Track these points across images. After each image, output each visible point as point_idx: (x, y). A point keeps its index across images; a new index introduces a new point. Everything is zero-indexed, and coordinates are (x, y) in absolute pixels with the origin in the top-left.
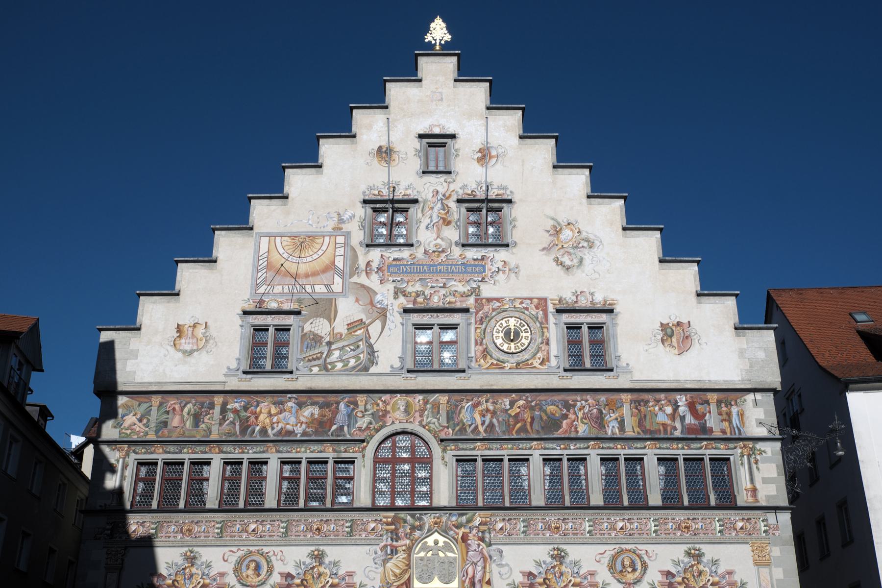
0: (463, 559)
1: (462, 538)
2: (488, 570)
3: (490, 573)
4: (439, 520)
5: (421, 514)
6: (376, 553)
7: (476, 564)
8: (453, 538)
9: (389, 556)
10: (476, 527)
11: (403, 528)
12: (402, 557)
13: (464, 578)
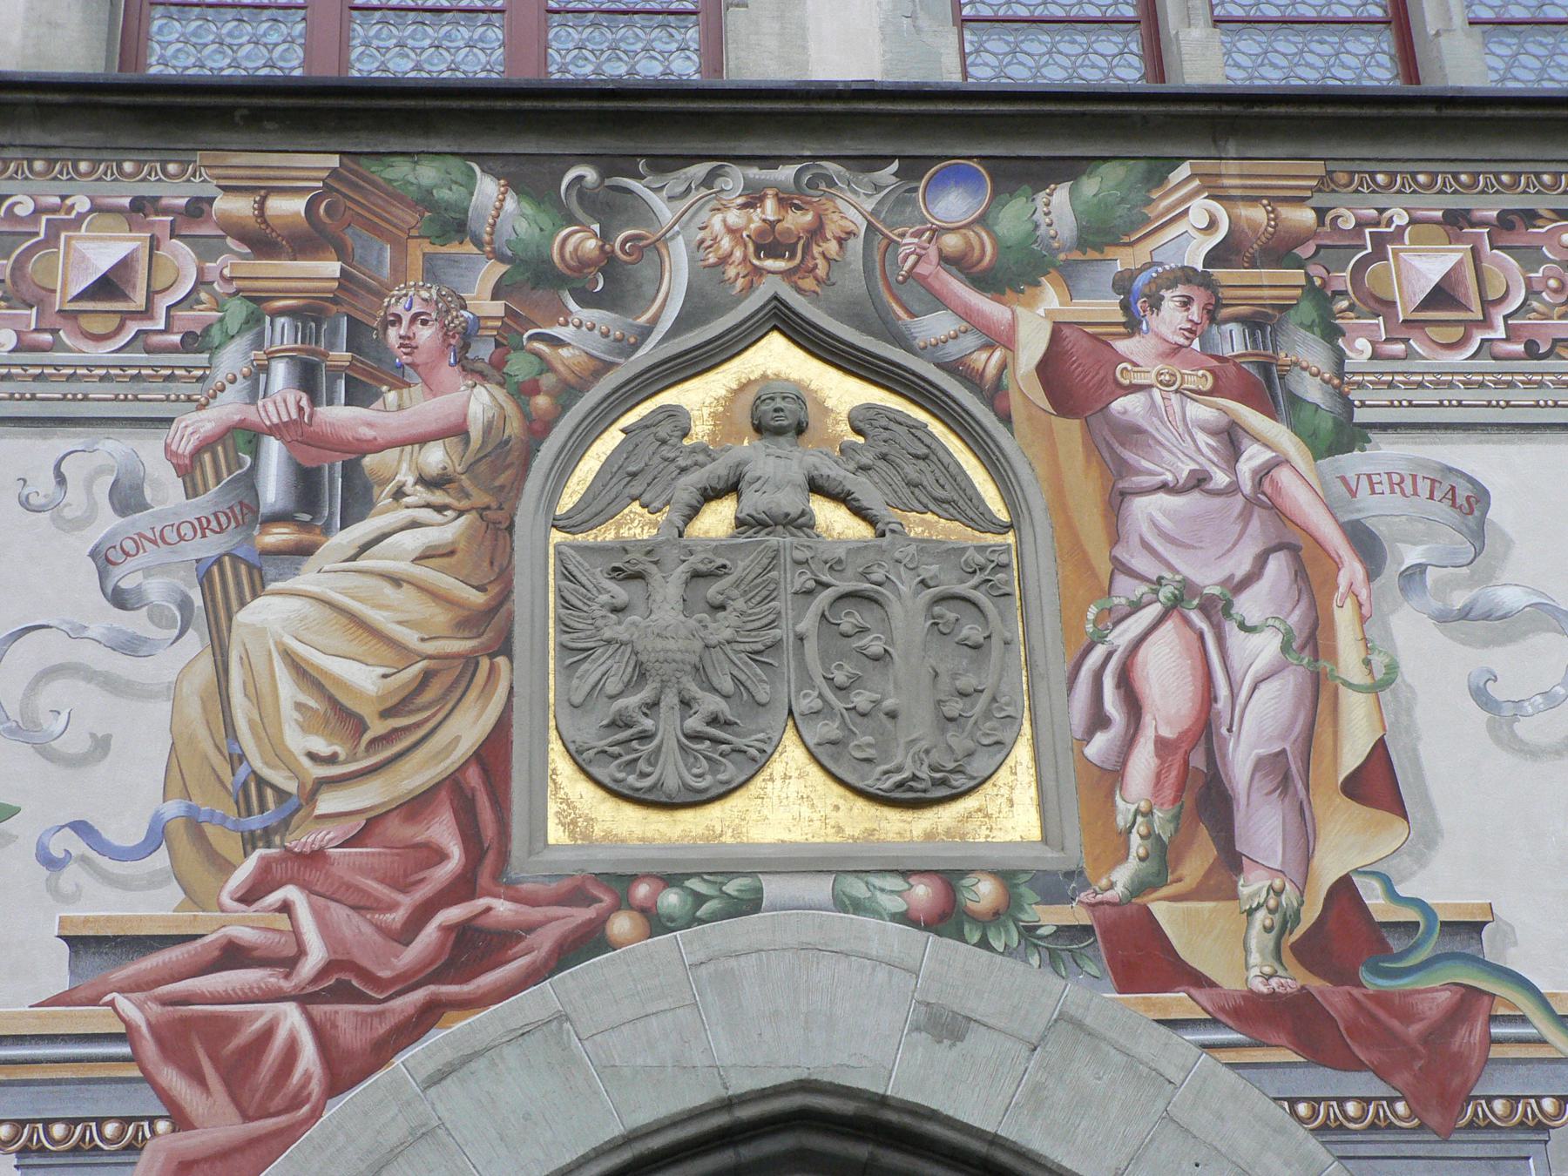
0: (1073, 552)
1: (1050, 369)
2: (1349, 660)
3: (1375, 688)
4: (797, 221)
5: (609, 165)
6: (127, 498)
7: (1217, 609)
8: (953, 368)
9: (279, 536)
10: (1186, 275)
11: (431, 273)
12: (412, 541)
13: (1099, 746)
